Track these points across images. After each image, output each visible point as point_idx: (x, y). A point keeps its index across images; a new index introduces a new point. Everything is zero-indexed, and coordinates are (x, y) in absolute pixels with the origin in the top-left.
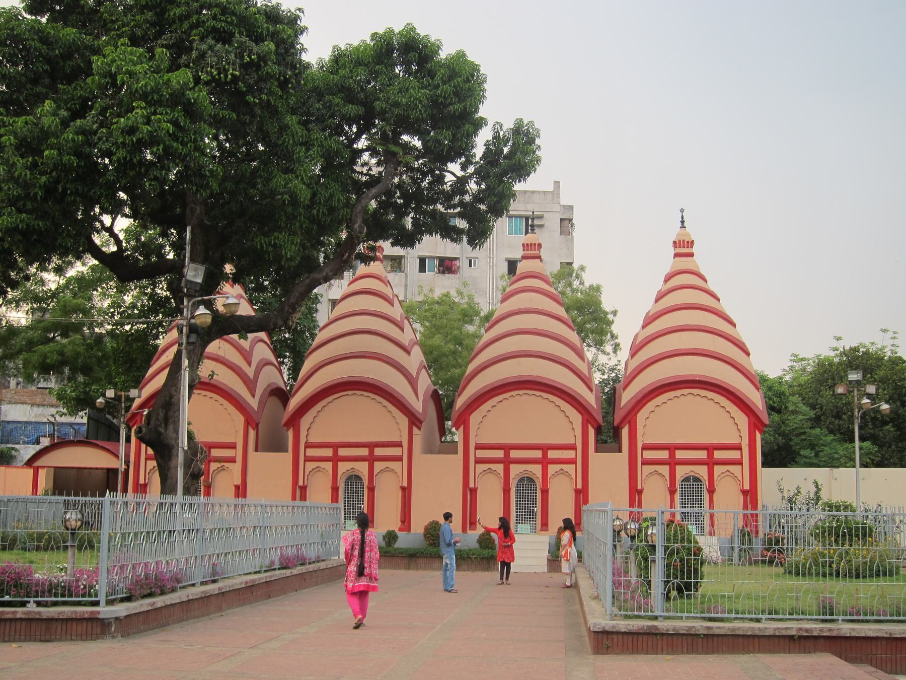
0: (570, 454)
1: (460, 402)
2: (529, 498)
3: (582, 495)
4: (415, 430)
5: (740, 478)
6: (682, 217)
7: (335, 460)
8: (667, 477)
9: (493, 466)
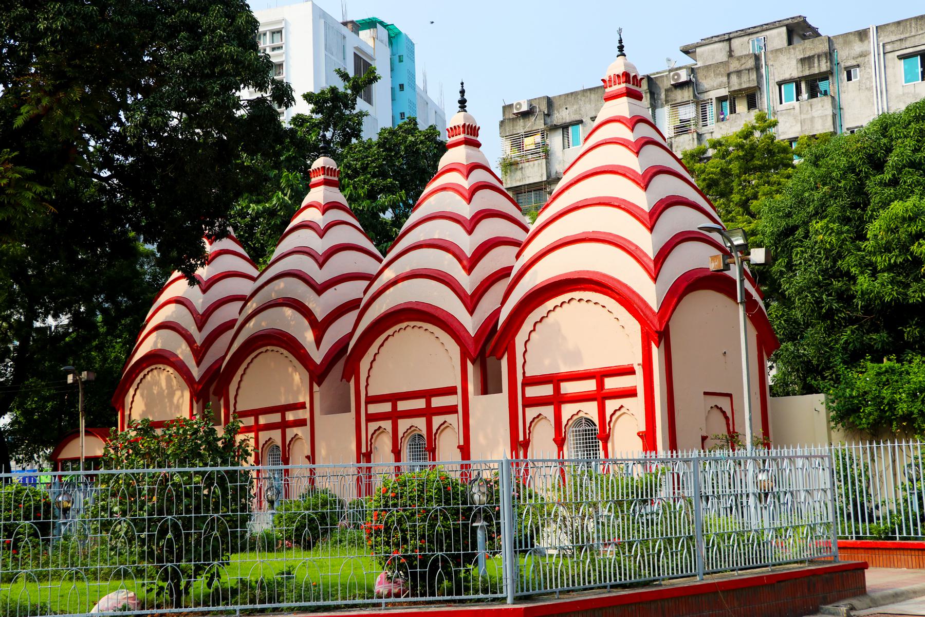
6: (620, 41)
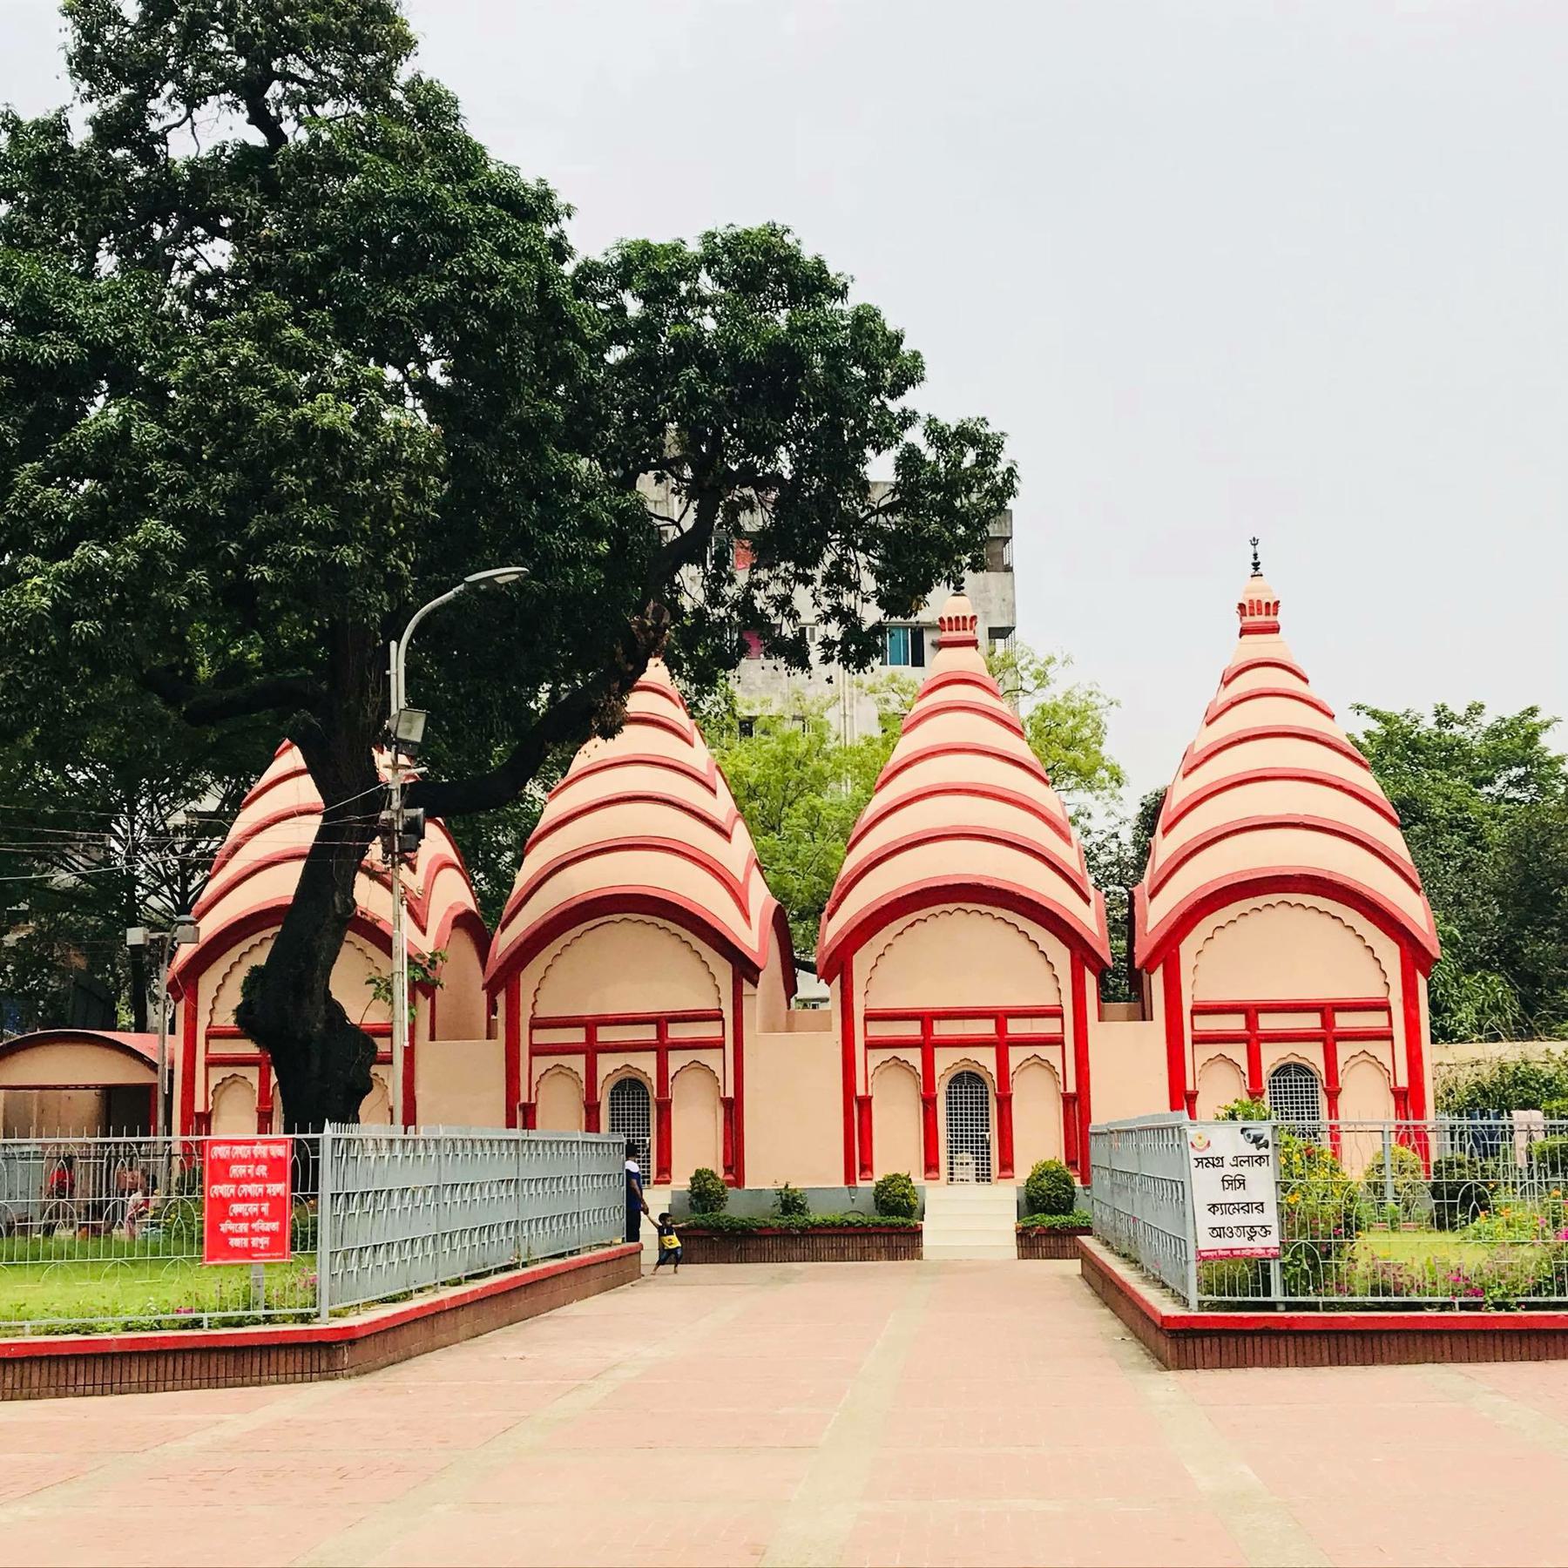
0: (1049, 1026)
1: (834, 928)
2: (971, 1115)
3: (1076, 1106)
4: (747, 988)
5: (1389, 1066)
6: (1255, 556)
7: (591, 1050)
8: (1245, 1068)
9: (903, 1054)
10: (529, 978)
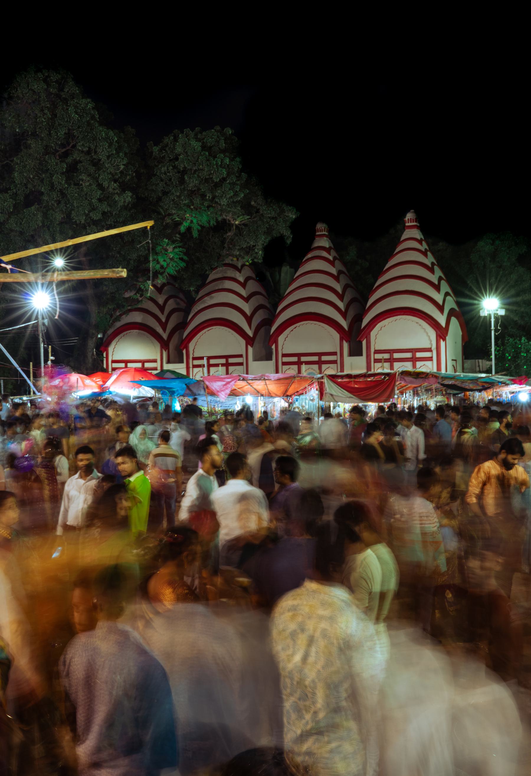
10: (191, 345)
